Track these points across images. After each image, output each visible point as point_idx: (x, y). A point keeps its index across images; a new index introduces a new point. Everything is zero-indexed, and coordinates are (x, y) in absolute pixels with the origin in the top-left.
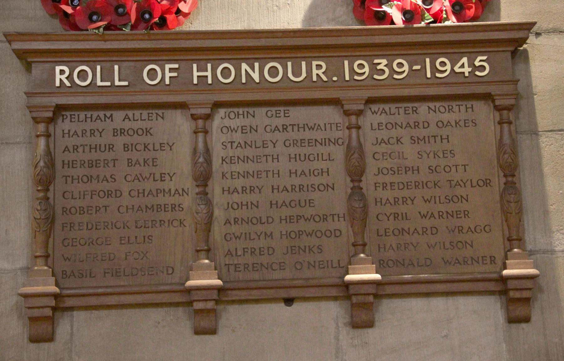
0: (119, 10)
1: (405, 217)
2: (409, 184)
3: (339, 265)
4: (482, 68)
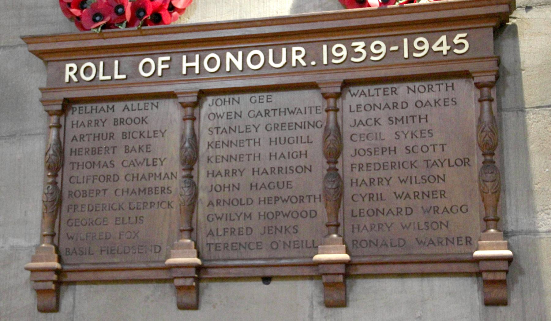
0: (118, 10)
1: (380, 197)
2: (386, 164)
3: (313, 245)
4: (462, 45)
